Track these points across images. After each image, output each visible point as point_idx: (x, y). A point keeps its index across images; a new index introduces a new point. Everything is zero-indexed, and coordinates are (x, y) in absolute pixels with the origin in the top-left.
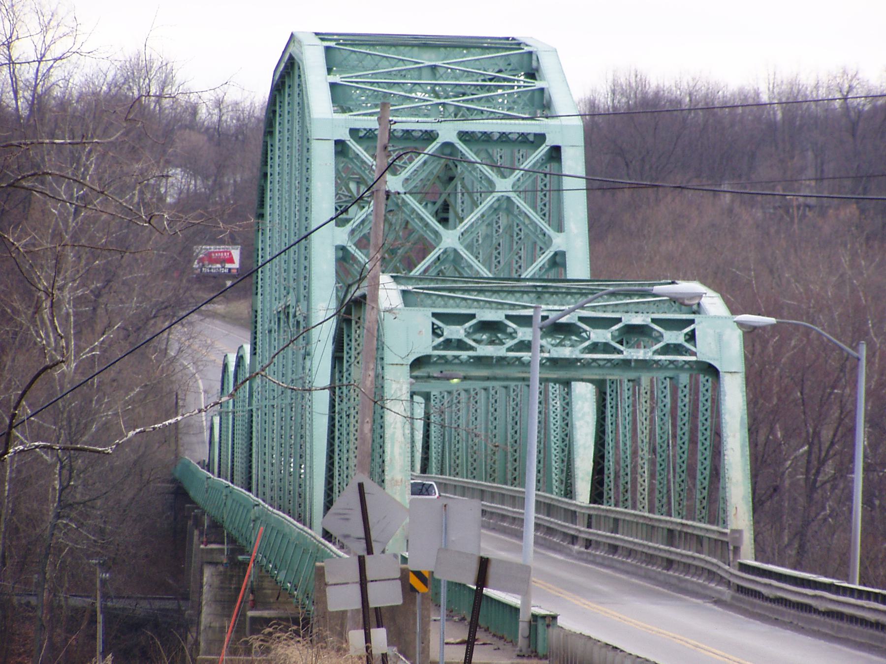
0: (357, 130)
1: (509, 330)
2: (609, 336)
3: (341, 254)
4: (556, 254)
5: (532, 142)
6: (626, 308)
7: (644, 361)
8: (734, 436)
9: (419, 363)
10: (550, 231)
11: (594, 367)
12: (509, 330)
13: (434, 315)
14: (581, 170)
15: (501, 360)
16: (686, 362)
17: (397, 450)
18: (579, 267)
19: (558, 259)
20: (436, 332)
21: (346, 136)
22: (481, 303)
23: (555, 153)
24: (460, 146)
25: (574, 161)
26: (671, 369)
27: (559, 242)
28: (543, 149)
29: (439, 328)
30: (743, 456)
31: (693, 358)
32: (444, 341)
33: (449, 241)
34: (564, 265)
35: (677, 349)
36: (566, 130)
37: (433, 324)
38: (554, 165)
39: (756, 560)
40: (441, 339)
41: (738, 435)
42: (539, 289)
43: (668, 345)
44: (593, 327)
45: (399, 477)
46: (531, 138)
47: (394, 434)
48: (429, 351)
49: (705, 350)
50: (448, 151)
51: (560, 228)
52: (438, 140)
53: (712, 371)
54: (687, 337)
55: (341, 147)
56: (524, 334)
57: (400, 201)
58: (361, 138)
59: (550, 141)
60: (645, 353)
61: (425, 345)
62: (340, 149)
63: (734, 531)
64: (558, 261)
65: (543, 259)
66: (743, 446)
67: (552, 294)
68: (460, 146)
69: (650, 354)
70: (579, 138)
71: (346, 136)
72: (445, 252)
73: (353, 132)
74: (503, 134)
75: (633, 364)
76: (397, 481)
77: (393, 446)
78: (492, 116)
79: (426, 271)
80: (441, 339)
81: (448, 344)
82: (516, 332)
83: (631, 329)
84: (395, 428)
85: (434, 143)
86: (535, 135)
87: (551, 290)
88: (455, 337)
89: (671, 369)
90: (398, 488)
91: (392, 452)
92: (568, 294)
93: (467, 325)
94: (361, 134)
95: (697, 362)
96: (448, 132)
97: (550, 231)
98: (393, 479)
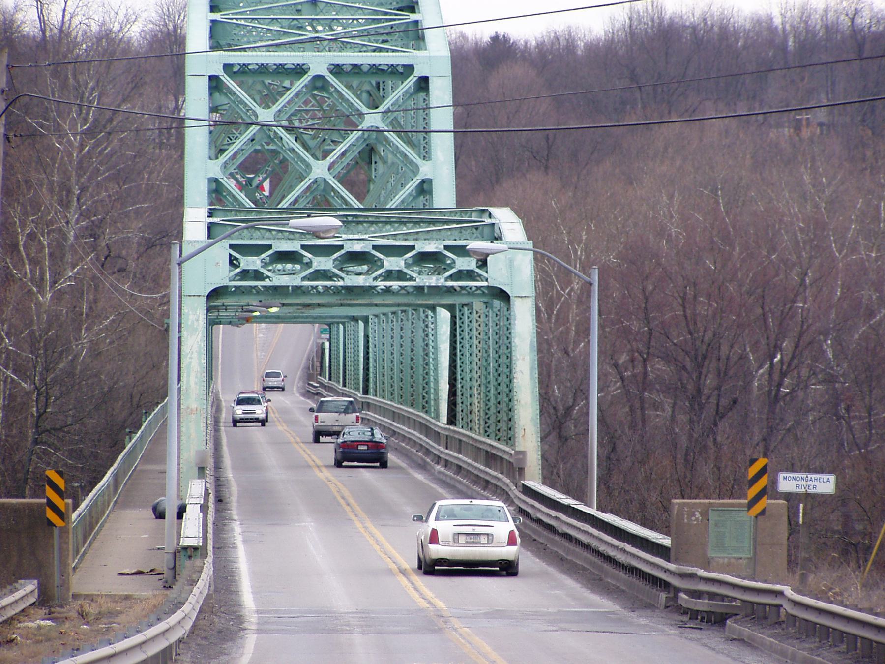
0: (232, 65)
1: (306, 260)
2: (402, 263)
3: (214, 186)
4: (423, 181)
5: (402, 73)
6: (415, 237)
7: (436, 287)
8: (524, 359)
9: (215, 294)
10: (418, 161)
11: (463, 294)
12: (306, 260)
13: (231, 246)
14: (448, 99)
15: (297, 289)
16: (478, 288)
17: (193, 380)
18: (445, 196)
19: (425, 186)
20: (233, 262)
21: (219, 71)
22: (274, 232)
23: (423, 83)
24: (331, 78)
25: (441, 92)
27: (425, 170)
28: (411, 81)
29: (236, 259)
31: (485, 284)
32: (240, 272)
33: (318, 171)
34: (430, 192)
35: (470, 275)
36: (434, 59)
37: (230, 255)
38: (422, 95)
39: (544, 483)
40: (238, 270)
41: (527, 358)
42: (350, 219)
43: (460, 272)
44: (387, 255)
45: (194, 406)
46: (401, 70)
47: (190, 363)
48: (226, 282)
49: (497, 275)
51: (426, 156)
53: (503, 296)
54: (480, 263)
59: (418, 72)
60: (437, 280)
61: (222, 276)
63: (518, 453)
64: (425, 188)
65: (412, 185)
66: (532, 369)
67: (372, 223)
68: (331, 78)
69: (442, 280)
70: (446, 69)
71: (219, 71)
72: (315, 181)
73: (227, 67)
74: (355, 66)
75: (426, 291)
76: (192, 410)
77: (188, 376)
79: (296, 201)
80: (238, 270)
81: (245, 274)
82: (311, 262)
83: (424, 257)
84: (191, 358)
85: (306, 76)
86: (404, 66)
87: (370, 219)
88: (251, 267)
90: (193, 416)
91: (188, 382)
92: (386, 223)
93: (263, 256)
94: (236, 69)
95: (488, 287)
96: (318, 63)
97: (418, 161)
98: (188, 408)
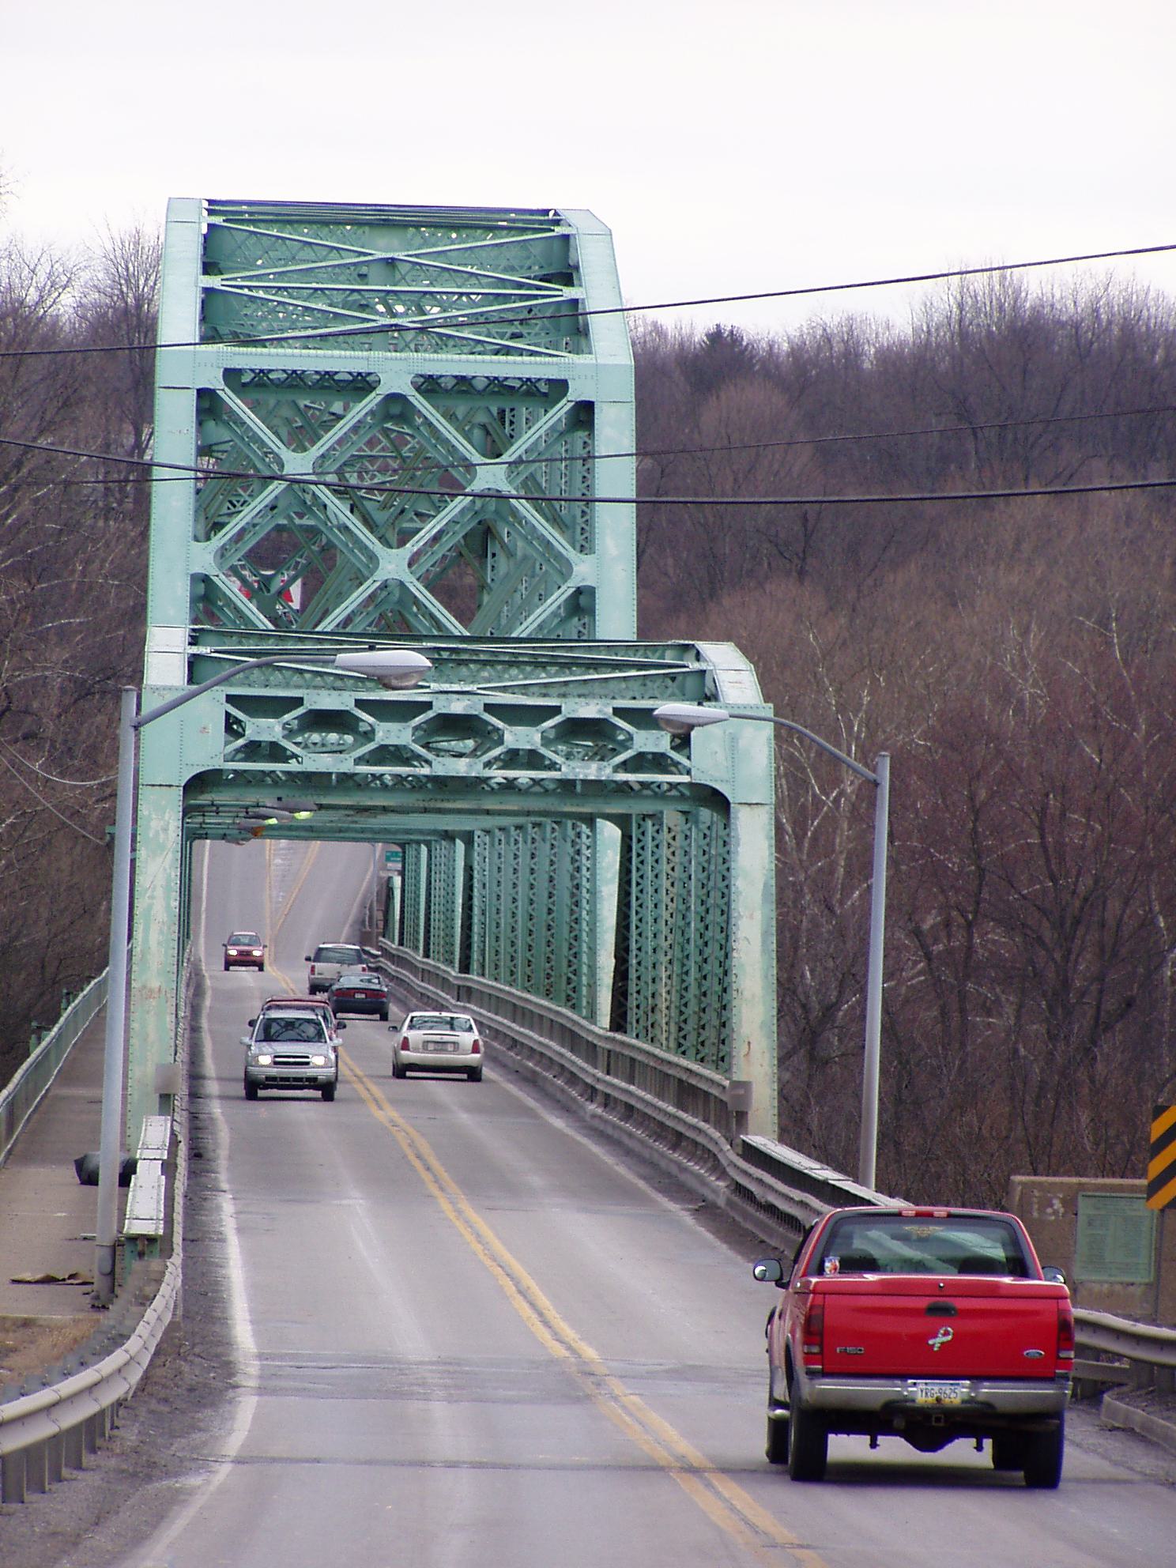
0: (239, 372)
1: (363, 727)
2: (538, 738)
3: (201, 588)
4: (579, 591)
5: (545, 394)
7: (597, 782)
8: (751, 917)
9: (199, 783)
10: (571, 554)
11: (647, 797)
12: (363, 727)
14: (629, 444)
15: (346, 778)
16: (673, 786)
17: (154, 937)
18: (617, 618)
19: (583, 600)
20: (232, 727)
21: (216, 382)
22: (308, 676)
23: (584, 414)
24: (419, 401)
25: (616, 429)
26: (536, 794)
27: (583, 571)
28: (562, 408)
29: (239, 722)
30: (764, 951)
31: (685, 779)
32: (245, 746)
33: (390, 567)
34: (591, 612)
35: (659, 762)
36: (603, 372)
37: (228, 715)
38: (581, 435)
40: (241, 742)
41: (758, 915)
42: (445, 655)
45: (155, 984)
46: (544, 388)
47: (150, 906)
48: (218, 763)
49: (706, 762)
50: (396, 409)
52: (378, 391)
53: (718, 801)
54: (678, 741)
55: (208, 404)
56: (518, 737)
57: (308, 498)
58: (244, 385)
59: (575, 394)
60: (600, 769)
61: (211, 750)
62: (206, 404)
64: (582, 603)
66: (765, 934)
67: (485, 663)
68: (419, 401)
69: (609, 770)
70: (626, 388)
71: (216, 382)
72: (385, 586)
73: (231, 375)
74: (461, 379)
75: (579, 788)
76: (151, 991)
77: (146, 930)
78: (479, 348)
79: (348, 620)
80: (241, 742)
81: (253, 750)
82: (373, 731)
83: (576, 728)
84: (152, 897)
85: (373, 394)
86: (549, 381)
87: (482, 657)
88: (265, 737)
89: (536, 794)
90: (154, 1003)
91: (146, 940)
92: (511, 664)
93: (287, 717)
94: (246, 378)
95: (691, 785)
97: (571, 554)
98: (144, 987)
